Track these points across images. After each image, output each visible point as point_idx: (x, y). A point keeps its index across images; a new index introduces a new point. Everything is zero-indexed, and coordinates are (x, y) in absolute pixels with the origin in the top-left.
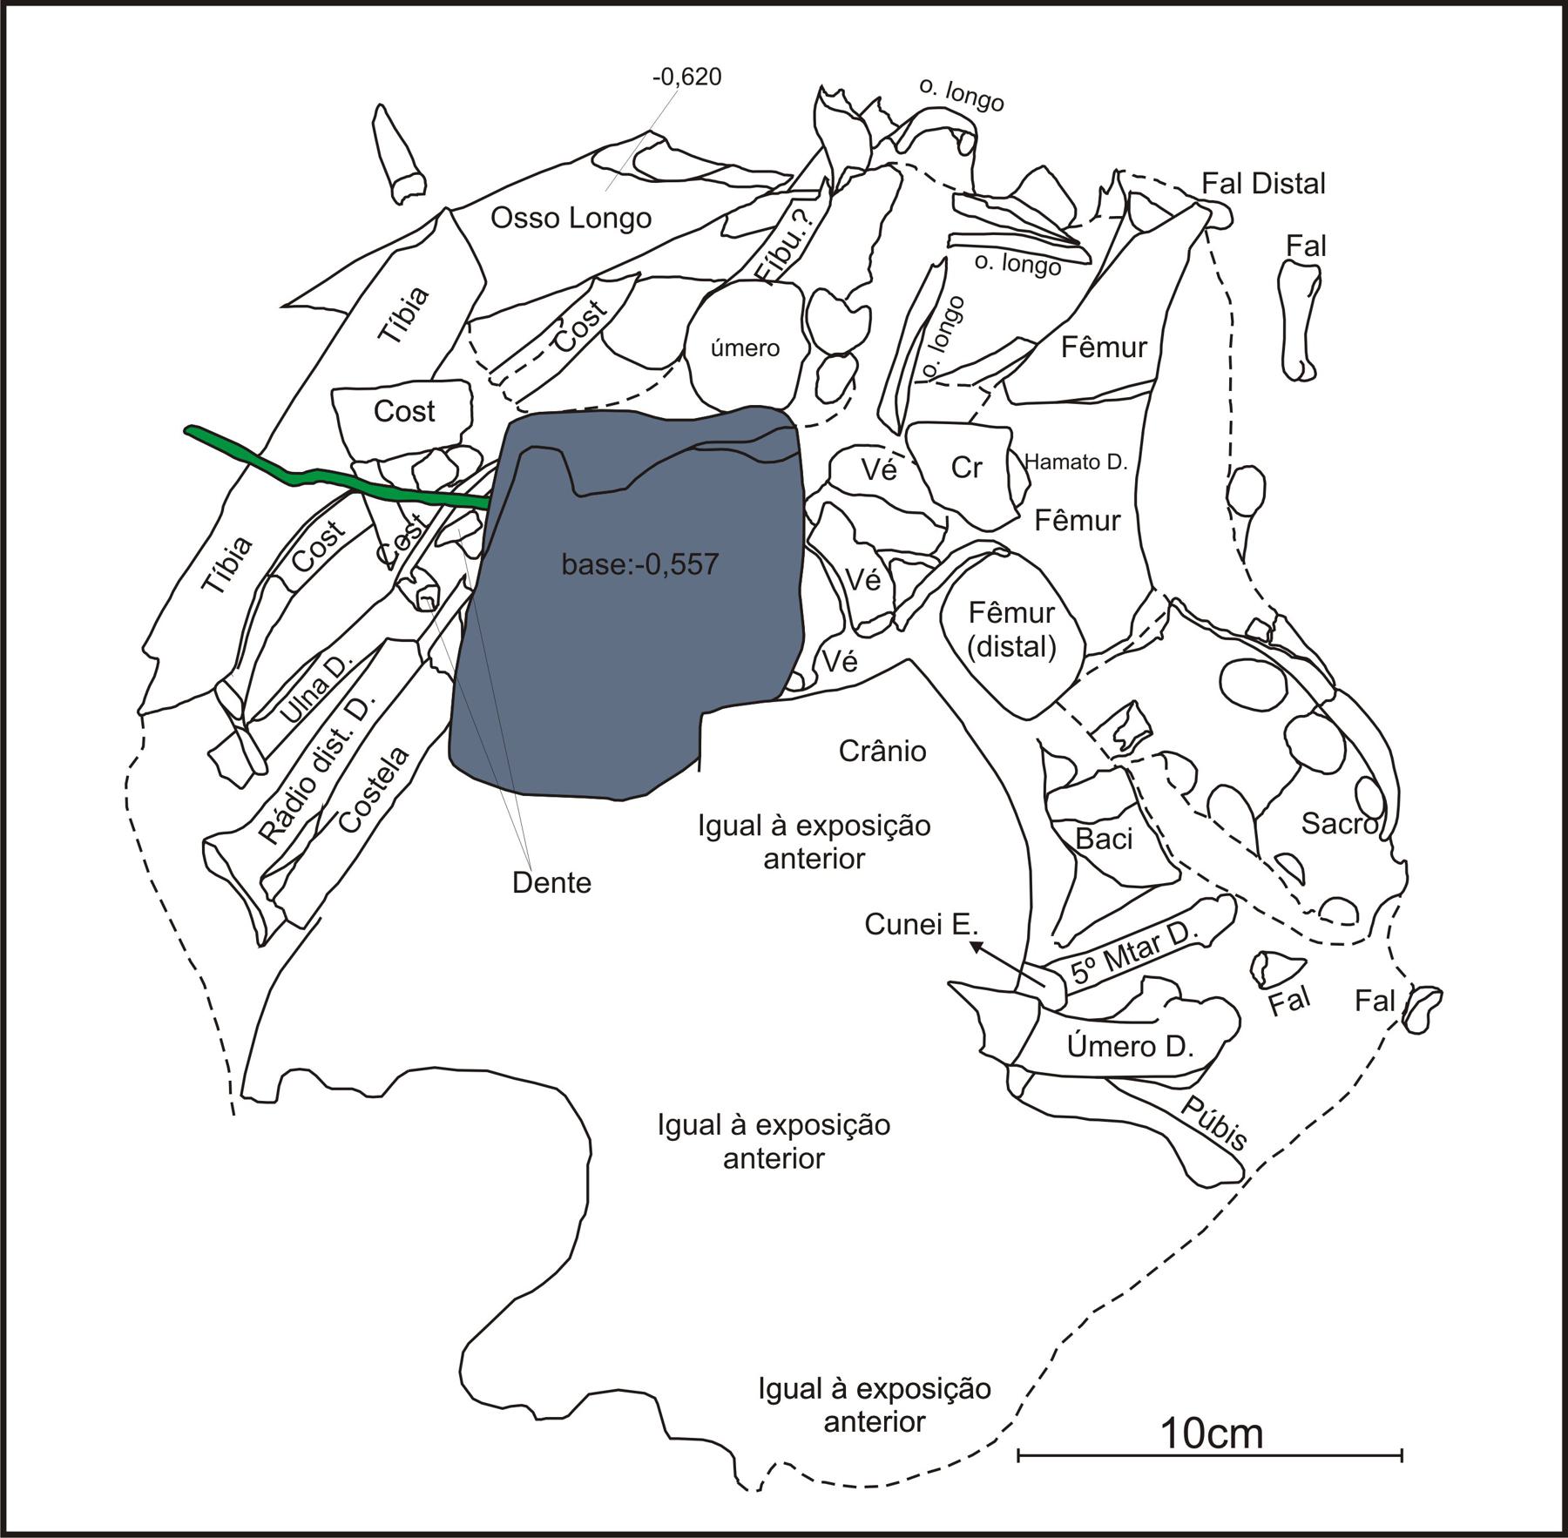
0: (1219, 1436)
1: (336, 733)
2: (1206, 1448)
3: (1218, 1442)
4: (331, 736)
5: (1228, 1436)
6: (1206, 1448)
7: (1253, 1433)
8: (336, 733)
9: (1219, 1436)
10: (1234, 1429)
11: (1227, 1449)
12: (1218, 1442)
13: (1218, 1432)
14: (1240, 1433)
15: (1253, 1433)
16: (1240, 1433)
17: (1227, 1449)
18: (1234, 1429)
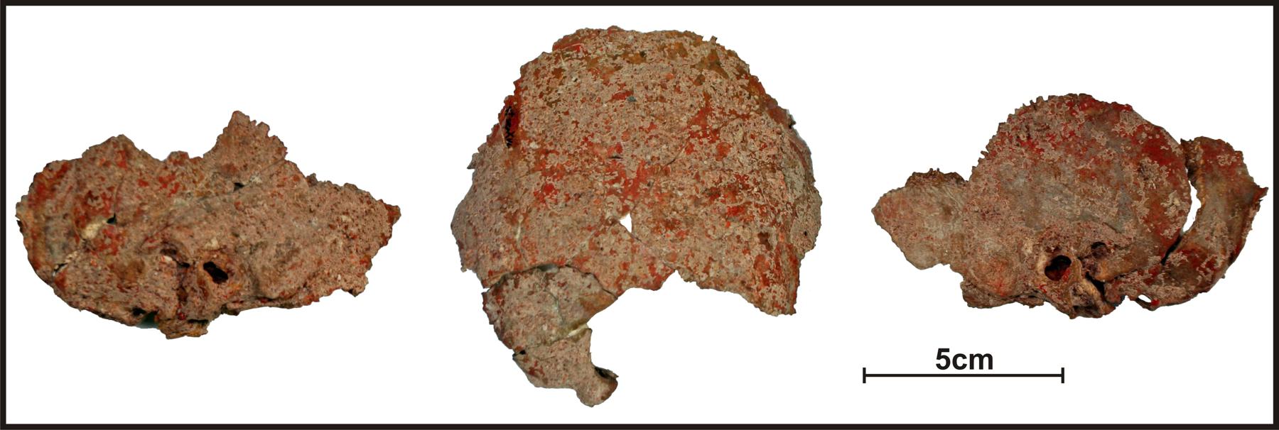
0: (960, 362)
2: (952, 370)
5: (967, 361)
6: (952, 370)
7: (986, 360)
9: (960, 362)
10: (972, 357)
11: (967, 371)
14: (977, 360)
15: (986, 360)
16: (977, 360)
17: (967, 371)
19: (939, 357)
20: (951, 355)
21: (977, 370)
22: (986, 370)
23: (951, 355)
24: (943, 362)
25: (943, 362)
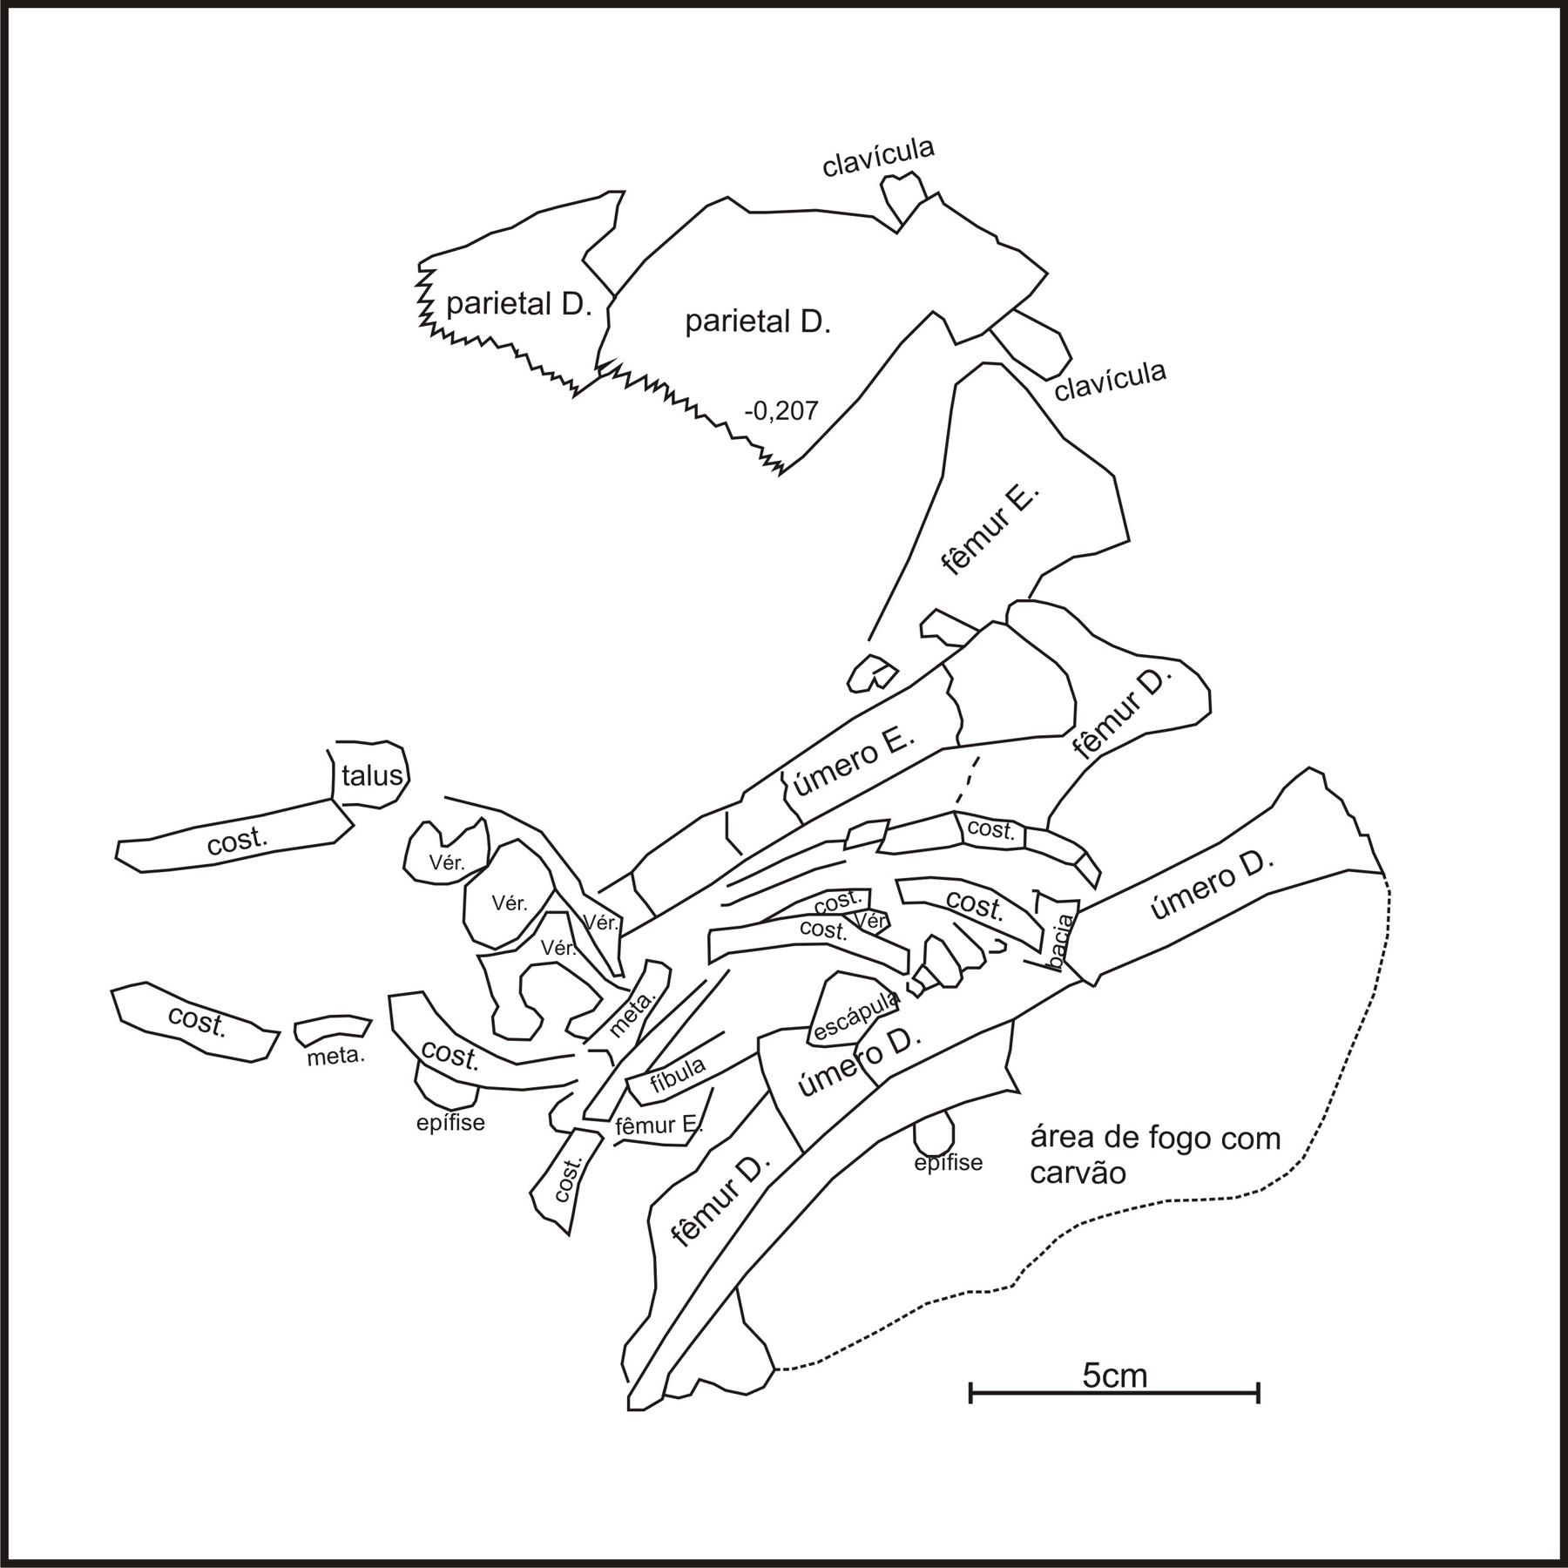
0: (1111, 1378)
1: (254, 832)
3: (1111, 1381)
4: (249, 832)
5: (1119, 1377)
7: (1140, 1375)
8: (254, 832)
9: (1111, 1378)
10: (1124, 1372)
11: (1119, 1388)
12: (1111, 1381)
13: (1111, 1375)
14: (1129, 1375)
15: (1140, 1375)
16: (1129, 1375)
18: (1124, 1372)
19: (1086, 1373)
20: (1101, 1370)
21: (1129, 1387)
22: (1140, 1387)
23: (1101, 1370)
24: (1092, 1379)
25: (1092, 1379)
